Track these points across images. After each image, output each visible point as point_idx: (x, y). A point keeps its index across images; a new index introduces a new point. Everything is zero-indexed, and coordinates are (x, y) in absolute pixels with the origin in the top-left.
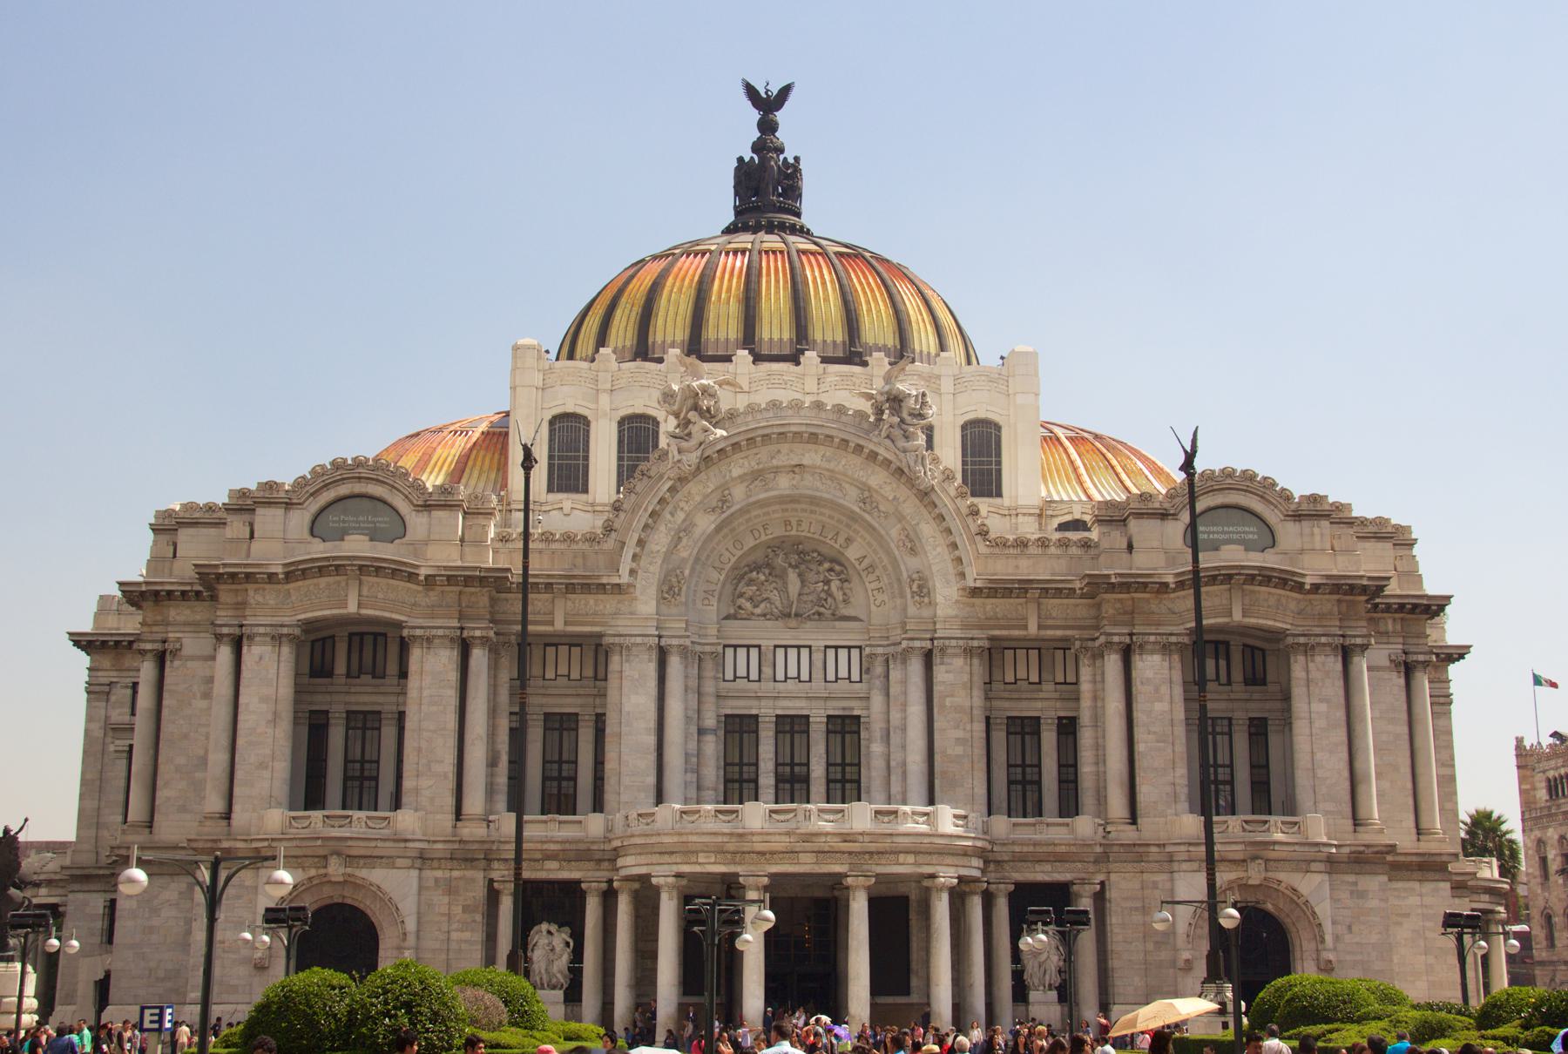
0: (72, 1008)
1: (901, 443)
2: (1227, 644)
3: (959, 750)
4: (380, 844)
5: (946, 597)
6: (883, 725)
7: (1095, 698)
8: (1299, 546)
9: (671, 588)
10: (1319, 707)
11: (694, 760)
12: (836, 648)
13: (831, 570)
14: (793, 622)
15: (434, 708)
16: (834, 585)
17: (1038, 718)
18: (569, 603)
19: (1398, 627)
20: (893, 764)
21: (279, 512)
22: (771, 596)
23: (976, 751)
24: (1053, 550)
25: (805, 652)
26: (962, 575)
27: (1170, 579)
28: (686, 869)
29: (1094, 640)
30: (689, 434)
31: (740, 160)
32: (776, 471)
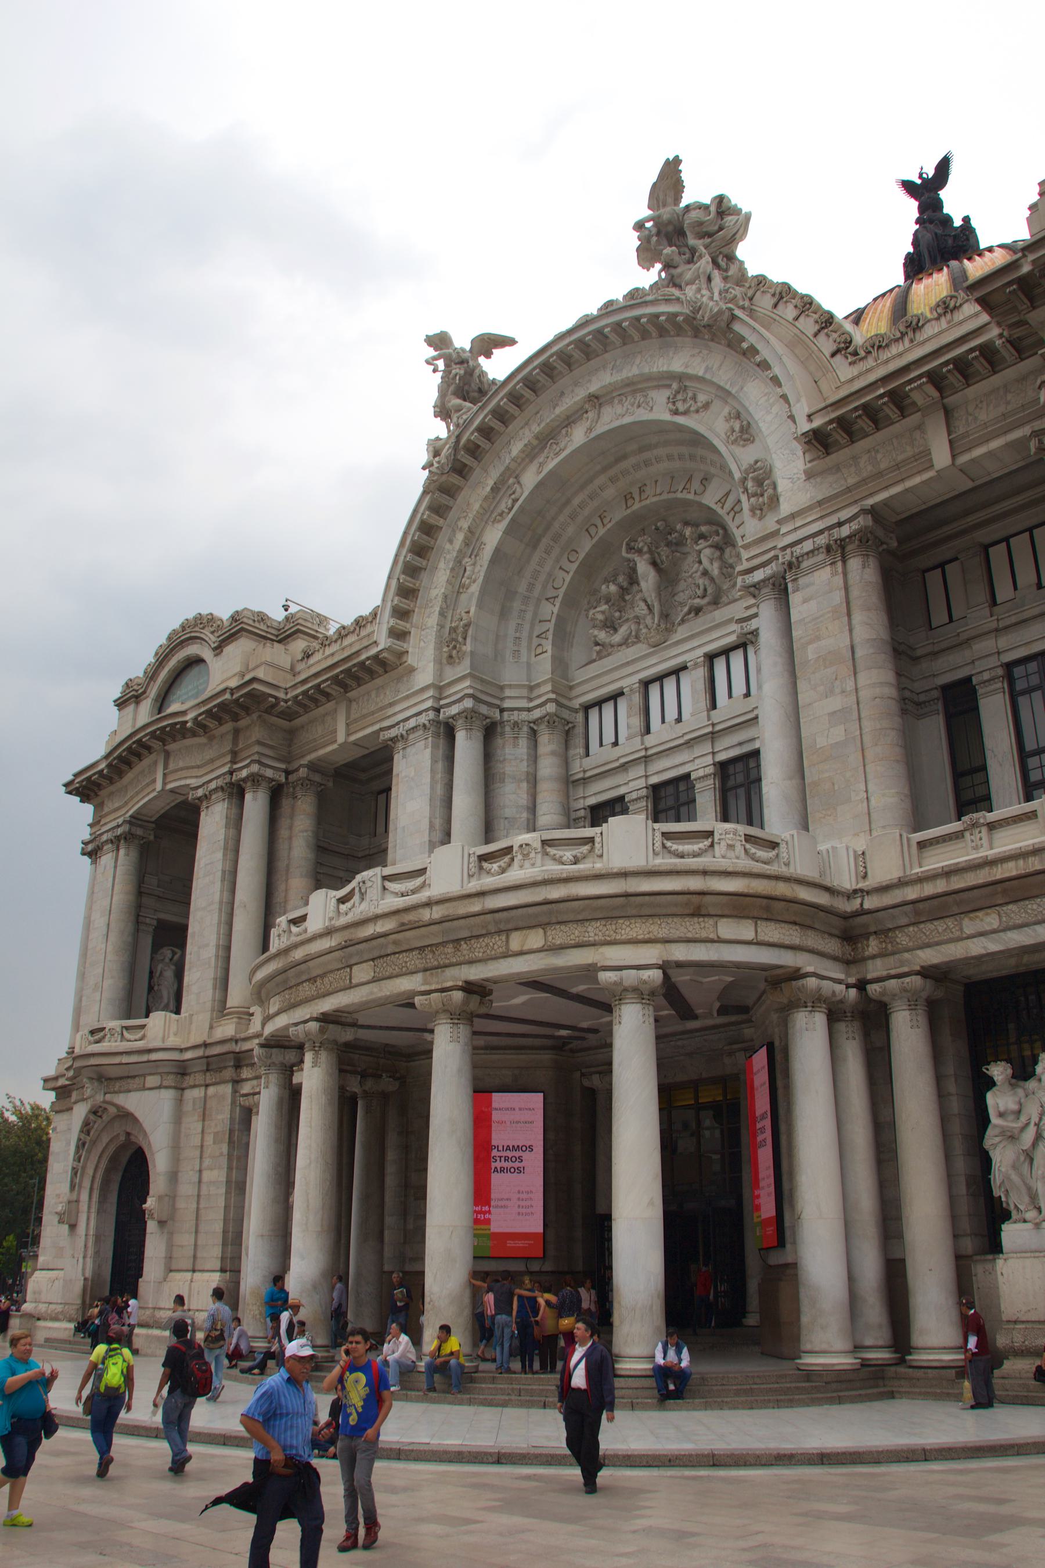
3: (838, 733)
4: (125, 1059)
12: (726, 652)
13: (702, 536)
18: (354, 705)
23: (867, 725)
32: (569, 421)
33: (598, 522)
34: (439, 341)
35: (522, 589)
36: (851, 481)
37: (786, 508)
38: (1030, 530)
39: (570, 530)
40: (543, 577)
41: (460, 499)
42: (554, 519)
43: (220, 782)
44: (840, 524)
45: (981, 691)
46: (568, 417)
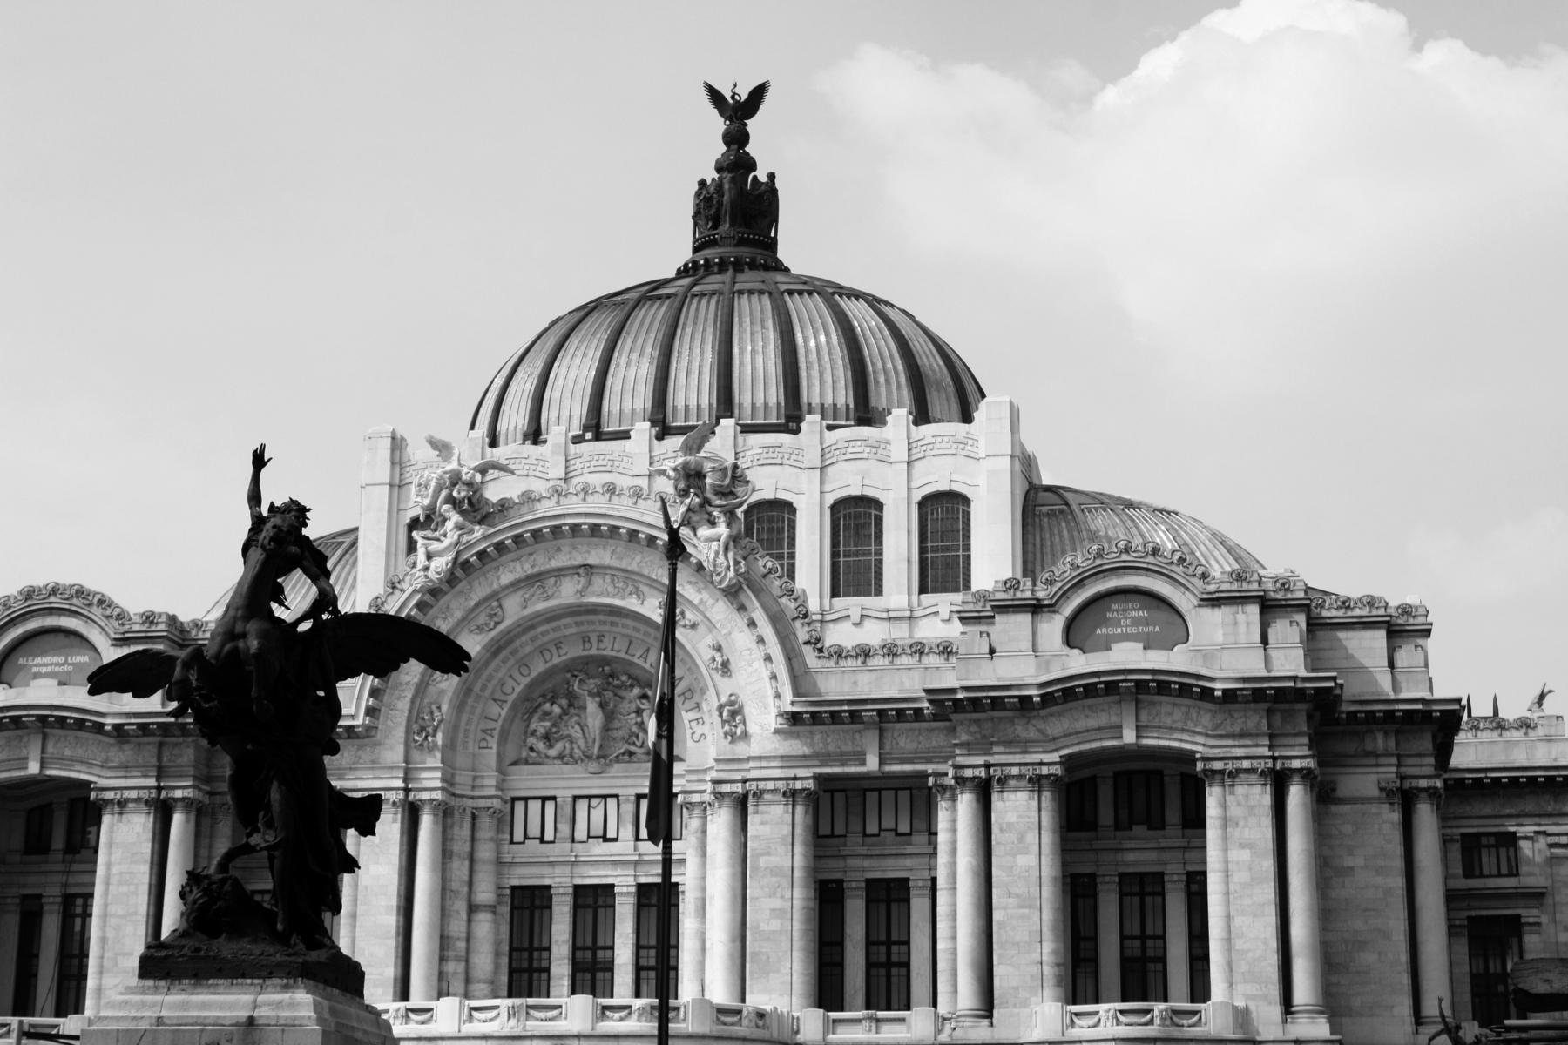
1: (704, 531)
2: (1160, 773)
3: (775, 925)
6: (699, 895)
8: (1219, 637)
9: (422, 729)
10: (1239, 855)
11: (462, 945)
14: (594, 766)
15: (124, 889)
17: (907, 880)
19: (1392, 743)
22: (572, 732)
24: (904, 660)
25: (612, 803)
26: (778, 696)
27: (1033, 692)
30: (445, 535)
31: (702, 183)
33: (554, 650)
35: (477, 688)
36: (807, 751)
37: (756, 747)
38: (896, 790)
39: (528, 649)
40: (495, 681)
41: (442, 602)
42: (517, 636)
43: (144, 794)
44: (795, 779)
45: (847, 893)
46: (559, 569)
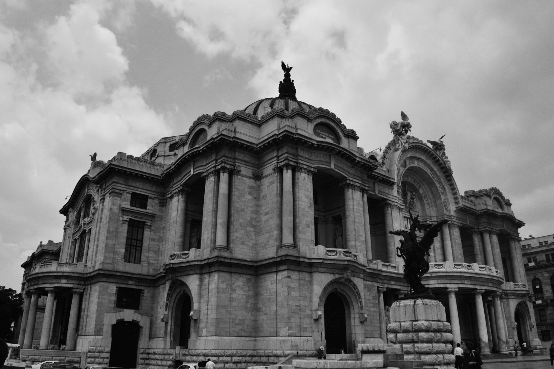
0: (101, 337)
5: (452, 208)
7: (480, 246)
15: (358, 214)
16: (415, 200)
20: (437, 260)
21: (306, 121)
28: (461, 286)
29: (479, 229)
31: (281, 82)
34: (404, 116)
